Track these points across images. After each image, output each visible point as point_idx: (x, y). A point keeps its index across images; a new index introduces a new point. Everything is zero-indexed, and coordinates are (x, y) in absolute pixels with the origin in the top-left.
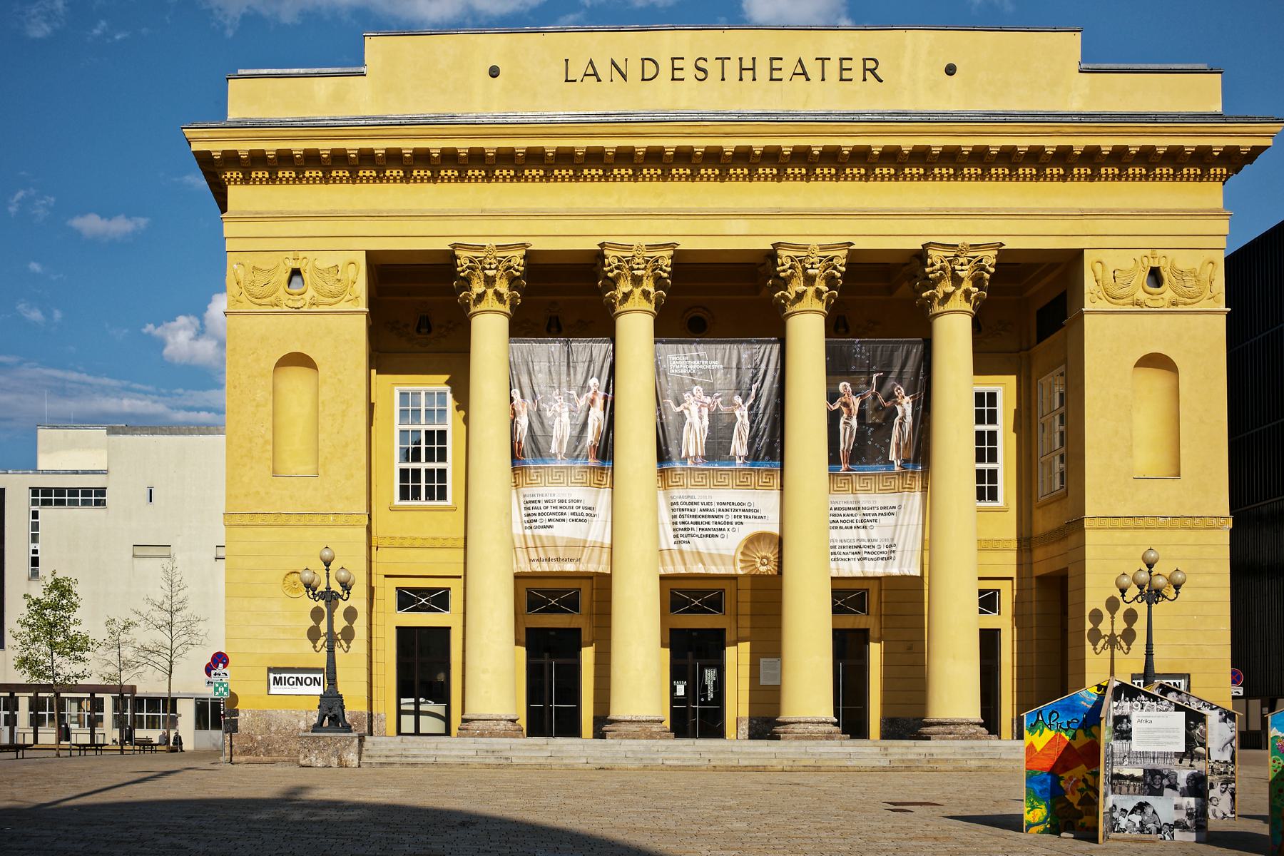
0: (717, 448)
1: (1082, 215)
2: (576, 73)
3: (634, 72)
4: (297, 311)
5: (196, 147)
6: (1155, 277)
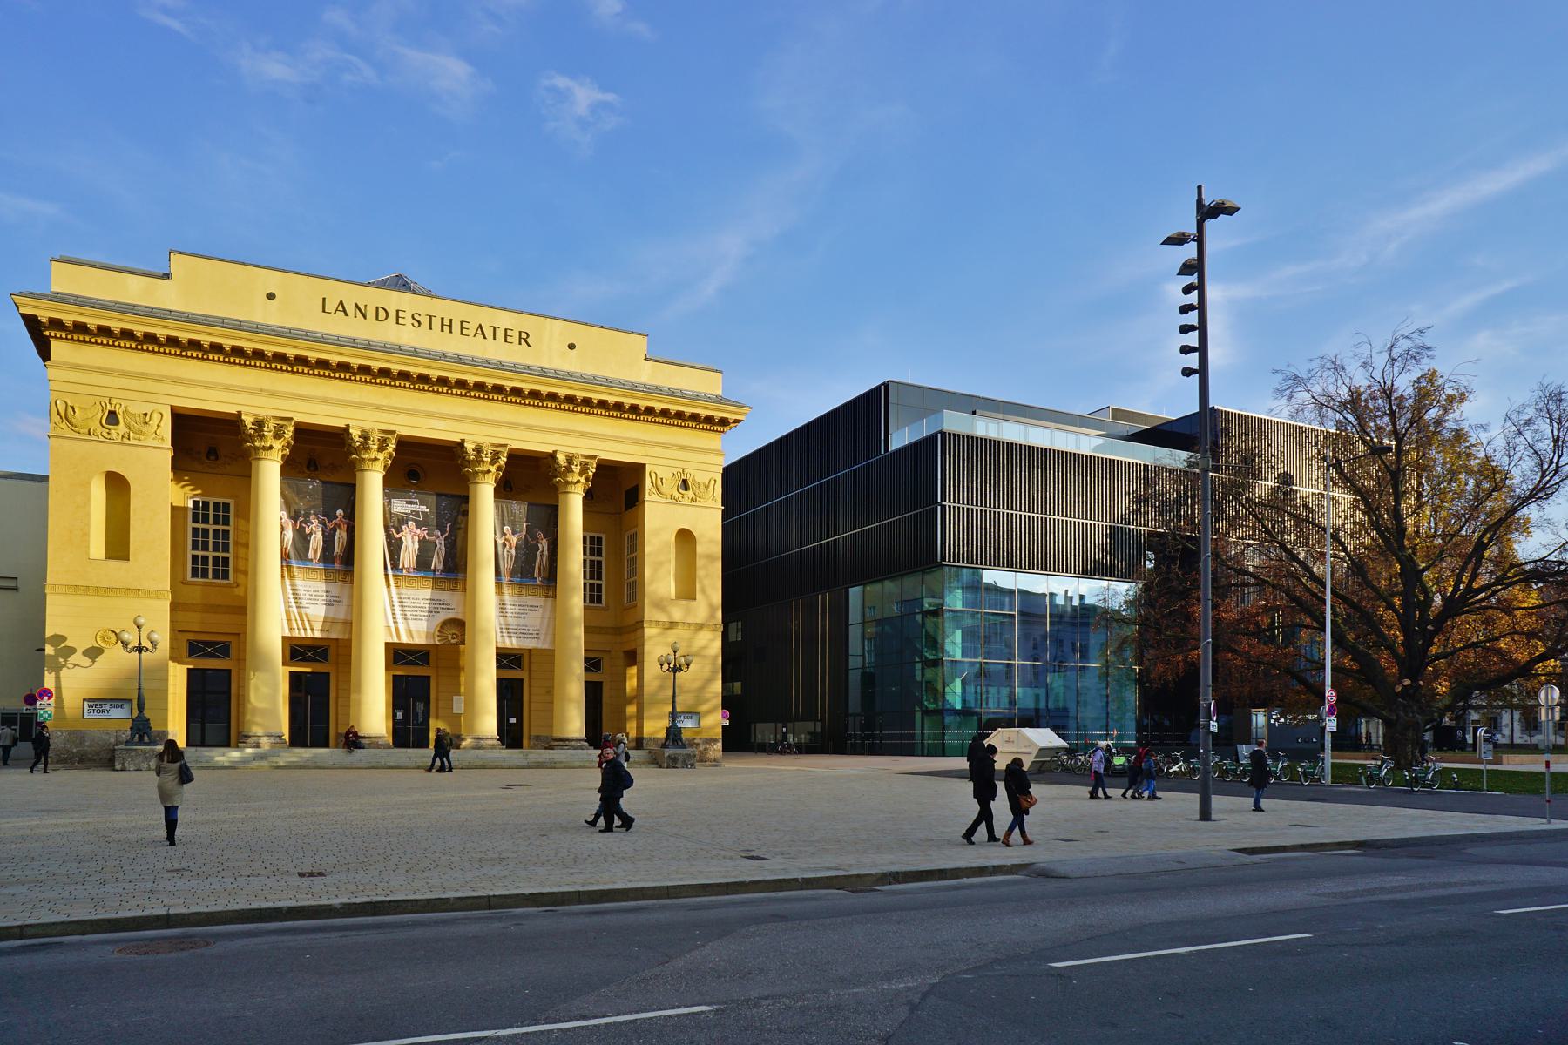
0: (422, 564)
1: (645, 443)
2: (330, 307)
3: (371, 313)
4: (110, 441)
5: (23, 310)
6: (685, 485)
